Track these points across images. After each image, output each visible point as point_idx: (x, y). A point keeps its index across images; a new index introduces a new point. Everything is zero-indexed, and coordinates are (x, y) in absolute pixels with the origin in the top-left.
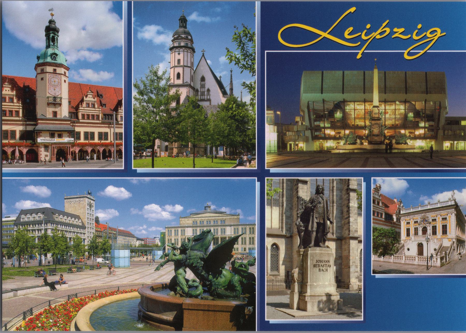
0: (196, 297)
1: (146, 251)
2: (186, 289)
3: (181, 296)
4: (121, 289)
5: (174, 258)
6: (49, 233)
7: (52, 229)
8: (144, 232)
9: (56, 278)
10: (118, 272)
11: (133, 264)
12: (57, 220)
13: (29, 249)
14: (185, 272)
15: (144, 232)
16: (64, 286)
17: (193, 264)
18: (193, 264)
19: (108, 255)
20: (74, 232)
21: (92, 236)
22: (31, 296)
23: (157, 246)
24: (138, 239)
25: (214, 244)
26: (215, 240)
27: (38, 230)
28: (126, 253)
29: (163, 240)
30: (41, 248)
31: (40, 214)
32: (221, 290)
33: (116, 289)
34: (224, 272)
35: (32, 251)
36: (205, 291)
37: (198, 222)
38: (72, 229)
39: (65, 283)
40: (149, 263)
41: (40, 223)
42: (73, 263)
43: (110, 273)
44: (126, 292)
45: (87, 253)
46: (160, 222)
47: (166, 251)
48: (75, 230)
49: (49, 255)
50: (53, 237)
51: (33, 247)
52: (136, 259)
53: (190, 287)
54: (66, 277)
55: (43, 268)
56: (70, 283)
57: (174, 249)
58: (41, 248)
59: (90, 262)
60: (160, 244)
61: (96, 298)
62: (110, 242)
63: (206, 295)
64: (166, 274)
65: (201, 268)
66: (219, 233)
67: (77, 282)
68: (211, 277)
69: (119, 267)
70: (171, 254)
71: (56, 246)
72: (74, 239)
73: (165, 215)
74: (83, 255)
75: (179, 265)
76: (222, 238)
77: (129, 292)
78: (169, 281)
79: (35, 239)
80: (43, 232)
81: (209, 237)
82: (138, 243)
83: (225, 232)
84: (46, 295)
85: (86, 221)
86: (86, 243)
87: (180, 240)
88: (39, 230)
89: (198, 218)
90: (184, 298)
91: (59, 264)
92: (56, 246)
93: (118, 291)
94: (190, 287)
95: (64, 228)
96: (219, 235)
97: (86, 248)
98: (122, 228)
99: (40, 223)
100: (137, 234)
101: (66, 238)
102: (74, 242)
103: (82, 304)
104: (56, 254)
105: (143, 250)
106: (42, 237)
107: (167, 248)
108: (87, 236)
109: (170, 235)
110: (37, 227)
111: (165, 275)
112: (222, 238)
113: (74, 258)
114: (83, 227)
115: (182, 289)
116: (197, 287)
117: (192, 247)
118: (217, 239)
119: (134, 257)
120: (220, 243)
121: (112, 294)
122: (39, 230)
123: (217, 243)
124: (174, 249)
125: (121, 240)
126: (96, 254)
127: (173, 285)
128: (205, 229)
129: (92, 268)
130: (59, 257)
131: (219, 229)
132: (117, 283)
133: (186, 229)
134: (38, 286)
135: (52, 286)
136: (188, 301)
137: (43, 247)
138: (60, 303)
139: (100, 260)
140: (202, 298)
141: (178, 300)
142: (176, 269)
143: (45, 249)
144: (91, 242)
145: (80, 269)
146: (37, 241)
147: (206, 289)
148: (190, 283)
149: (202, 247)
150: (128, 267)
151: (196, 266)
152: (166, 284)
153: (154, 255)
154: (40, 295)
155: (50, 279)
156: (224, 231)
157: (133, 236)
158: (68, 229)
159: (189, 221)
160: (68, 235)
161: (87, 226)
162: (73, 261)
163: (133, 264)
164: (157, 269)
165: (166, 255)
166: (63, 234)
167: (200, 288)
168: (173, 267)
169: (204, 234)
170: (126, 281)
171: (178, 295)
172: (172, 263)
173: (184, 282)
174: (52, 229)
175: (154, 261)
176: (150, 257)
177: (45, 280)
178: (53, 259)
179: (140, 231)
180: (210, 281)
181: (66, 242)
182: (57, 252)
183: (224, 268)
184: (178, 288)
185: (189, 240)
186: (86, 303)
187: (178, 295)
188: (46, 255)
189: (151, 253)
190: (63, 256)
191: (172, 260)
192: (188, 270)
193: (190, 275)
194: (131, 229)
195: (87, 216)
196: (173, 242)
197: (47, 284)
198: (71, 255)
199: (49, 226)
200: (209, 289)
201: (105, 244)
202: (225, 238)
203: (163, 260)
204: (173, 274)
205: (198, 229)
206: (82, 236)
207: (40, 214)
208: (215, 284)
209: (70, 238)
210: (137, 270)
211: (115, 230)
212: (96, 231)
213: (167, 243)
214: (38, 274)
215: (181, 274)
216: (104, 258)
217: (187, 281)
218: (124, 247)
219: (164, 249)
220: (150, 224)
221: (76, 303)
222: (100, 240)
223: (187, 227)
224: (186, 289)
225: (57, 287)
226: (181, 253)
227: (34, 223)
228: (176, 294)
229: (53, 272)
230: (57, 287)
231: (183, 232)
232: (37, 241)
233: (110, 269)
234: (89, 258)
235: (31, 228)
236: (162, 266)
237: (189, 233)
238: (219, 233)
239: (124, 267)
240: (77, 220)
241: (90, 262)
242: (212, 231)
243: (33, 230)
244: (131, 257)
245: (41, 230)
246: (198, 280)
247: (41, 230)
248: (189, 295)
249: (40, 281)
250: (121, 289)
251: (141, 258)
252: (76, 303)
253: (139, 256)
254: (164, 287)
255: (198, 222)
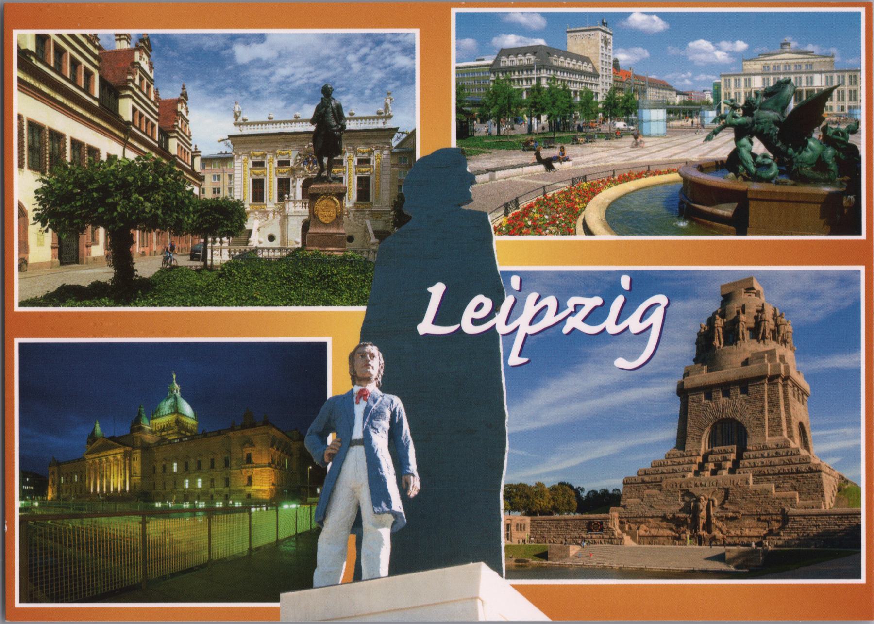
0: (768, 180)
1: (691, 112)
2: (753, 169)
3: (745, 179)
4: (652, 169)
5: (734, 121)
6: (544, 83)
7: (548, 79)
8: (688, 82)
9: (554, 152)
10: (648, 142)
11: (671, 131)
12: (555, 63)
13: (513, 109)
14: (751, 143)
15: (688, 82)
16: (566, 164)
17: (763, 130)
18: (763, 130)
19: (632, 117)
20: (582, 83)
21: (609, 88)
22: (516, 179)
23: (707, 104)
24: (678, 93)
25: (796, 100)
26: (798, 94)
27: (527, 79)
28: (660, 114)
29: (717, 95)
30: (531, 107)
31: (529, 56)
32: (807, 170)
33: (646, 169)
34: (811, 143)
35: (517, 111)
36: (781, 173)
37: (771, 67)
38: (578, 78)
39: (567, 160)
40: (695, 129)
41: (529, 68)
42: (580, 129)
43: (637, 145)
44: (660, 173)
45: (600, 115)
46: (711, 67)
47: (722, 111)
48: (583, 79)
49: (544, 118)
50: (550, 90)
51: (520, 105)
52: (676, 123)
53: (758, 165)
54: (570, 150)
55: (534, 137)
56: (574, 159)
57: (734, 107)
58: (531, 107)
59: (605, 128)
60: (712, 100)
61: (615, 182)
62: (637, 97)
63: (783, 179)
64: (722, 147)
65: (775, 137)
66: (804, 84)
67: (585, 158)
68: (790, 150)
69: (650, 136)
70: (729, 117)
71: (554, 103)
72: (581, 93)
73: (720, 56)
74: (596, 117)
75: (741, 132)
76: (807, 92)
77: (666, 173)
78: (726, 156)
79: (521, 94)
80: (534, 82)
81: (789, 90)
82: (678, 99)
83: (812, 83)
84: (538, 177)
85: (599, 66)
86: (600, 99)
87: (743, 94)
88: (529, 80)
89: (771, 61)
90: (749, 183)
91: (559, 131)
92: (554, 103)
93: (649, 171)
94: (758, 165)
95: (566, 76)
96: (804, 86)
97: (600, 106)
98: (654, 77)
99: (529, 68)
100: (677, 85)
101: (569, 92)
102: (581, 97)
103: (594, 191)
104: (555, 117)
105: (687, 110)
106: (532, 90)
107: (723, 106)
108: (601, 90)
109: (728, 86)
110: (525, 75)
111: (718, 147)
112: (807, 92)
113: (580, 122)
114: (595, 75)
115: (746, 168)
116: (769, 166)
117: (761, 104)
118: (801, 92)
119: (672, 120)
120: (804, 98)
121: (639, 176)
122: (529, 80)
123: (801, 99)
124: (734, 107)
125: (652, 94)
126: (615, 116)
127: (733, 162)
128: (782, 77)
129: (608, 136)
130: (558, 120)
131: (804, 77)
132: (646, 159)
133: (753, 78)
134: (527, 165)
135: (548, 164)
136: (755, 186)
137: (534, 105)
138: (559, 191)
139: (620, 125)
140: (777, 183)
141: (740, 185)
142: (738, 139)
143: (536, 109)
144: (607, 98)
145: (590, 139)
146: (525, 96)
147: (784, 168)
148: (759, 159)
149: (777, 104)
150: (663, 136)
151: (768, 134)
152: (722, 161)
153: (703, 118)
154: (529, 178)
155: (545, 154)
156: (810, 81)
157: (670, 88)
158: (572, 77)
159: (758, 66)
160: (573, 87)
161: (600, 73)
162: (579, 126)
163: (671, 131)
164: (708, 139)
165: (722, 118)
166: (564, 86)
167: (775, 167)
168: (732, 136)
169: (781, 85)
170: (660, 157)
171: (740, 178)
172: (732, 129)
173: (749, 158)
174: (548, 79)
175: (703, 126)
176: (696, 121)
177: (538, 156)
178: (550, 123)
179: (683, 80)
180: (790, 156)
181: (570, 97)
182: (555, 112)
183: (810, 137)
184: (741, 168)
185: (757, 94)
186: (599, 191)
187: (740, 178)
188: (539, 118)
189: (697, 114)
190: (564, 119)
191: (731, 125)
192: (755, 140)
193: (759, 147)
194: (668, 78)
195: (600, 59)
196: (733, 97)
197: (540, 160)
198: (576, 118)
199: (544, 73)
200: (790, 170)
201: (627, 101)
202: (813, 91)
203: (717, 125)
204: (732, 146)
205: (771, 78)
206: (594, 89)
207: (529, 56)
208: (797, 162)
209: (576, 92)
210: (677, 140)
211: (643, 79)
212: (615, 81)
213: (723, 99)
214: (527, 146)
215: (744, 146)
216: (627, 121)
217: (754, 156)
218: (657, 106)
219: (719, 108)
220: (697, 70)
221: (585, 188)
222: (622, 95)
223: (754, 75)
224: (753, 169)
225: (556, 165)
226: (744, 115)
227: (521, 68)
228: (737, 177)
229: (549, 143)
230: (556, 165)
231: (748, 83)
232: (525, 96)
233: (636, 138)
234: (604, 121)
235: (516, 76)
236: (715, 133)
237: (757, 83)
238: (804, 84)
239: (658, 136)
240: (585, 64)
241: (605, 128)
242: (793, 80)
243: (518, 80)
244: (668, 120)
245: (531, 79)
246: (771, 155)
247: (531, 79)
248: (757, 178)
249: (531, 157)
250: (652, 169)
251: (683, 122)
252: (585, 188)
253: (680, 119)
254: (718, 166)
255: (771, 67)
